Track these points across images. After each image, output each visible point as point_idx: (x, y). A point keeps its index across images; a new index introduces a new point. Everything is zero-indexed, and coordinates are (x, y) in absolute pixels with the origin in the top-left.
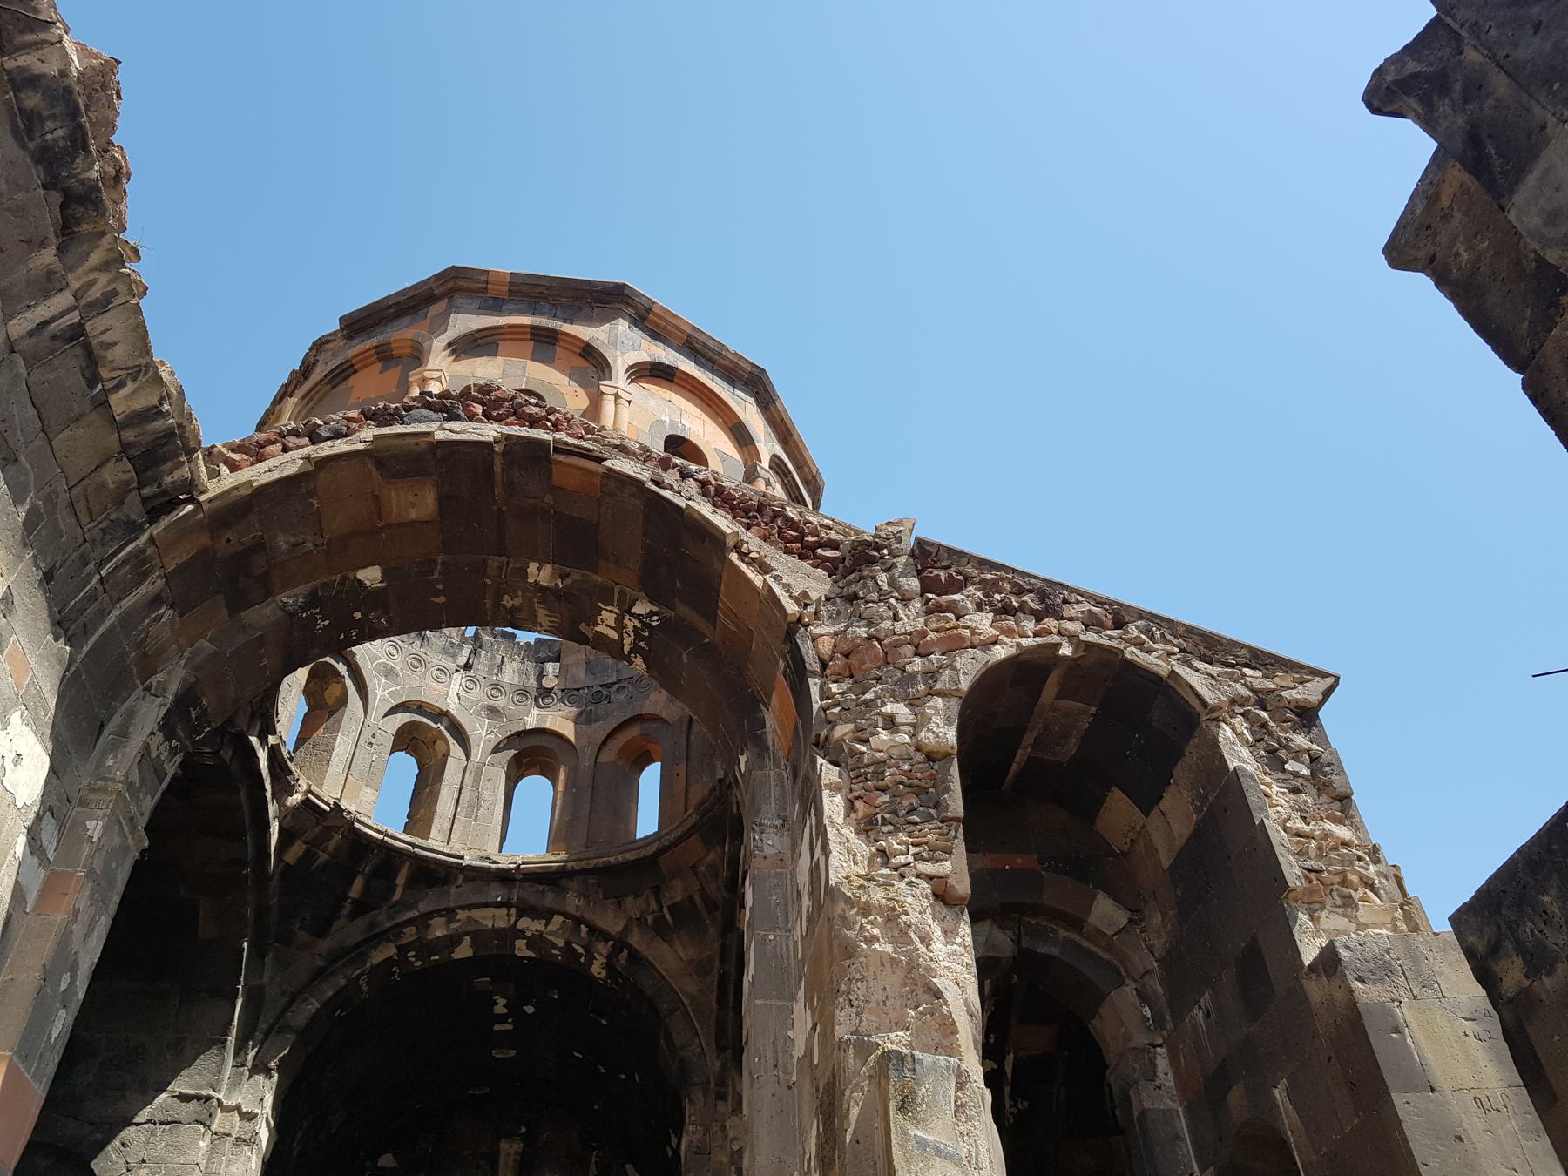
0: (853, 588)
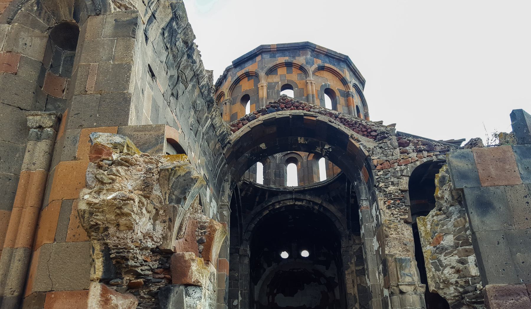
0: (381, 145)
